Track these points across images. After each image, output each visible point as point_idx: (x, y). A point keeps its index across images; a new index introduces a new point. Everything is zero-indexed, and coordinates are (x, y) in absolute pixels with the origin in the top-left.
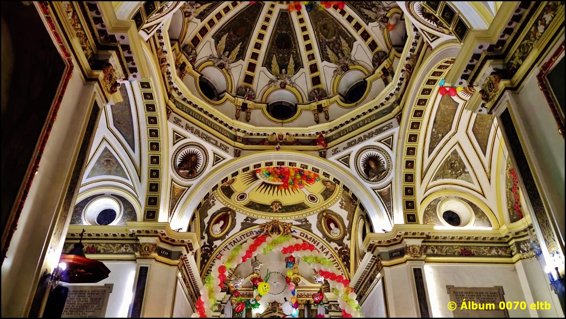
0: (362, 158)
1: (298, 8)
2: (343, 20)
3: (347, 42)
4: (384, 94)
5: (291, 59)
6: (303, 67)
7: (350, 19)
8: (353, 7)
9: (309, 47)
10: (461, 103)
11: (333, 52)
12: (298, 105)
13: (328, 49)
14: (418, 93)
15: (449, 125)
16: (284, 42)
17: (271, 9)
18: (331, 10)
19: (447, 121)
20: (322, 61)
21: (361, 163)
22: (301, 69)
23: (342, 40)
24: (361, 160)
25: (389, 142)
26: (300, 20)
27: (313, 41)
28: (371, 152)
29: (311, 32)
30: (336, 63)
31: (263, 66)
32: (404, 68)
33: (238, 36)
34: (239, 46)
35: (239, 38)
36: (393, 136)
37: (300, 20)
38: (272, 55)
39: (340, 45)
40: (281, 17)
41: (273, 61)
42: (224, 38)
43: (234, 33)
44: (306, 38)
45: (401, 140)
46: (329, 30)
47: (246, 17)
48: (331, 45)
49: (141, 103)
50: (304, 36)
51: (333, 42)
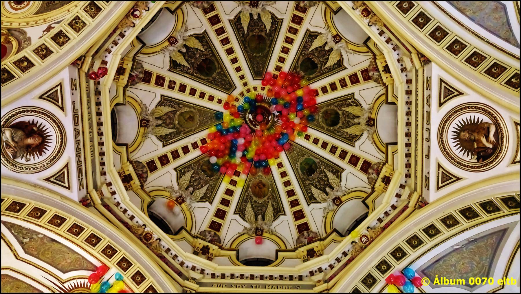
0: (48, 125)
1: (227, 106)
2: (188, 141)
4: (117, 183)
5: (186, 64)
6: (169, 70)
7: (186, 150)
8: (196, 161)
9: (182, 88)
10: (64, 277)
11: (164, 115)
12: (141, 45)
14: (127, 254)
15: (36, 253)
17: (244, 81)
18: (204, 134)
19: (43, 254)
20: (162, 96)
21: (40, 121)
22: (168, 67)
23: (171, 131)
24: (45, 123)
25: (60, 178)
27: (185, 97)
28: (53, 145)
29: (195, 100)
30: (153, 113)
31: (205, 31)
33: (253, 36)
34: (245, 28)
35: (251, 34)
36: (68, 188)
39: (167, 126)
40: (229, 83)
41: (200, 44)
42: (268, 26)
43: (260, 37)
45: (57, 199)
46: (186, 121)
47: (260, 56)
48: (171, 115)
50: (195, 90)
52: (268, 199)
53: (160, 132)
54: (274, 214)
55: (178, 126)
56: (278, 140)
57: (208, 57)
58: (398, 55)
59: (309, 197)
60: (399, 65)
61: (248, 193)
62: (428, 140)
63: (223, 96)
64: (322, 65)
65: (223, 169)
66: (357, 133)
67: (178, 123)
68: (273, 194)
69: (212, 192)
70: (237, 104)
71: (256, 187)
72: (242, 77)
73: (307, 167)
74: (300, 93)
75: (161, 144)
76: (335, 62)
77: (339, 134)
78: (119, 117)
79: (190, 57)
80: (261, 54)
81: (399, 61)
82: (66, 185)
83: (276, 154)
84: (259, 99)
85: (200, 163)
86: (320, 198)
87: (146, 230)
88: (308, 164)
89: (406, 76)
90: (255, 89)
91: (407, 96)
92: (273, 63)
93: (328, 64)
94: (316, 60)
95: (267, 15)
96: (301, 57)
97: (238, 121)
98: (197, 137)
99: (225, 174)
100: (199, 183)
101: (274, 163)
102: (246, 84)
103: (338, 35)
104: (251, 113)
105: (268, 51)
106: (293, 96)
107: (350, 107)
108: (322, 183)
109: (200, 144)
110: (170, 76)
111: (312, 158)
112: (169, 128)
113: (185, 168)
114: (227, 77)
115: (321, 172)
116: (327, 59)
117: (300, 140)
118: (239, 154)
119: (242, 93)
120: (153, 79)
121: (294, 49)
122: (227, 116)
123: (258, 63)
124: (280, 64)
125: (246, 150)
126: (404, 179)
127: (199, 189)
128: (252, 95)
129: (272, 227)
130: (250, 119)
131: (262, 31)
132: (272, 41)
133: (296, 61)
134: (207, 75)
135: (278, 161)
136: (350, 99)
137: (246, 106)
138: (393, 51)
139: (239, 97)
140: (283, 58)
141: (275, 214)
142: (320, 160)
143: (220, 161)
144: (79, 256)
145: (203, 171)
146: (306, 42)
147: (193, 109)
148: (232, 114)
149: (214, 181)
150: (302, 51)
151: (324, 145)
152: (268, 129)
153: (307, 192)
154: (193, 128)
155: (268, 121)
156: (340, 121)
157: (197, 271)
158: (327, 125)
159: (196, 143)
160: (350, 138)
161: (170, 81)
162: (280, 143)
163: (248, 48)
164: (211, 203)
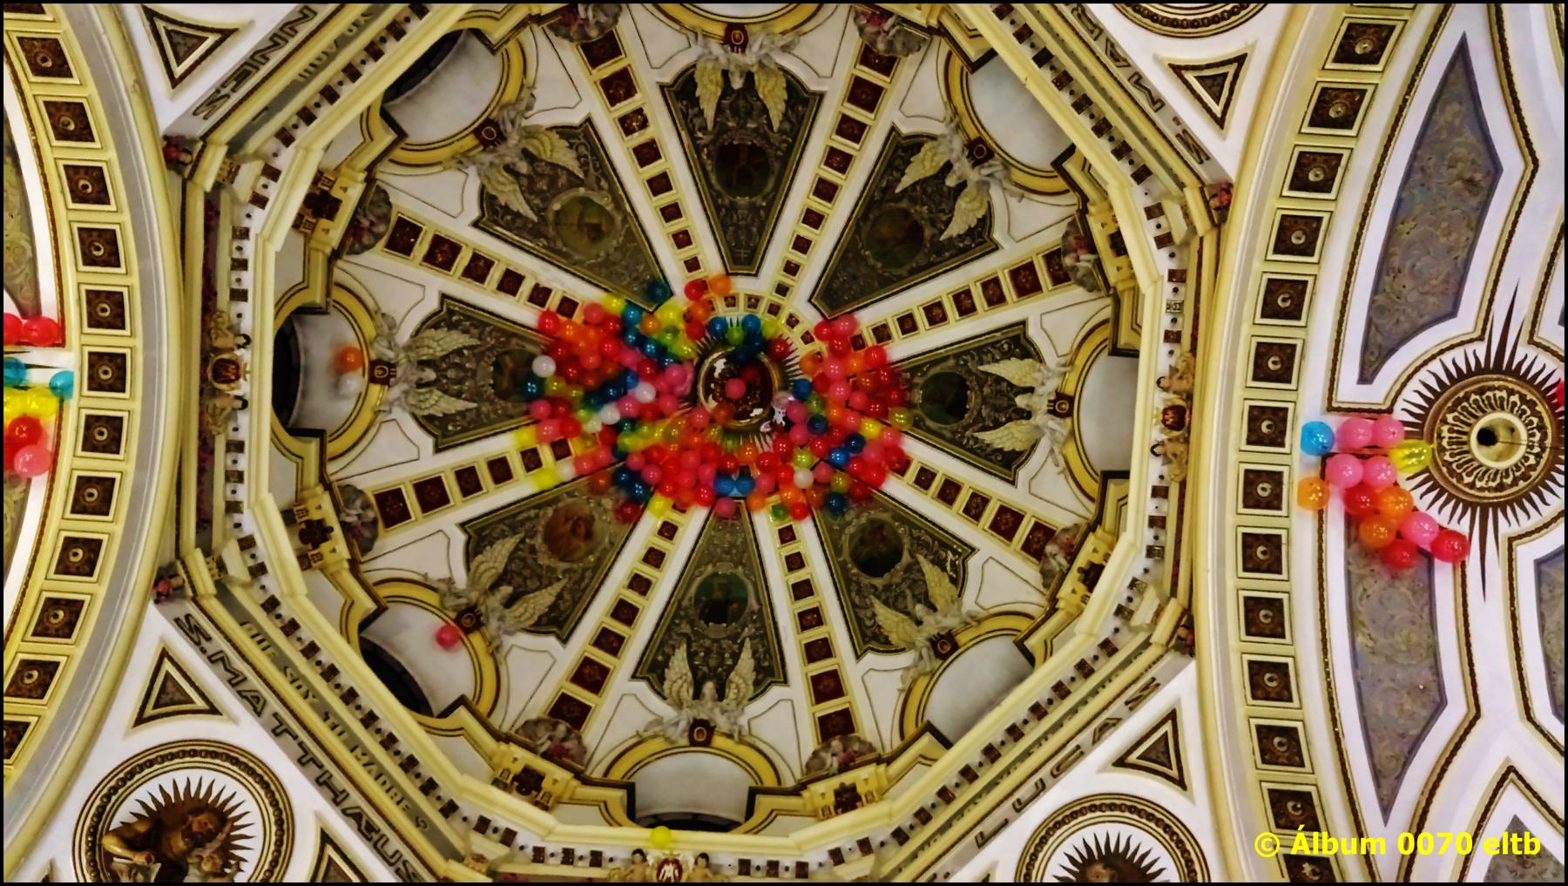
1: (697, 289)
2: (536, 270)
3: (506, 208)
4: (293, 185)
5: (709, 111)
6: (662, 87)
8: (506, 330)
9: (646, 153)
11: (548, 164)
13: (573, 165)
14: (140, 359)
16: (744, 161)
17: (787, 280)
18: (585, 293)
20: (589, 120)
22: (668, 80)
23: (525, 210)
26: (689, 242)
29: (646, 207)
30: (531, 133)
31: (821, 96)
32: (244, 355)
33: (906, 213)
34: (907, 181)
35: (904, 204)
36: (175, 82)
37: (689, 242)
38: (787, 126)
39: (529, 190)
40: (754, 250)
41: (782, 107)
42: (956, 228)
43: (916, 229)
44: (660, 184)
45: (123, 77)
46: (580, 225)
47: (873, 268)
48: (563, 180)
49: (1326, 274)
50: (668, 188)
51: (560, 191)
52: (565, 572)
53: (501, 188)
54: (540, 617)
55: (550, 216)
56: (722, 474)
57: (770, 151)
58: (1146, 571)
59: (654, 661)
60: (1127, 593)
61: (537, 516)
62: (1020, 807)
63: (712, 263)
64: (975, 423)
65: (542, 408)
66: (893, 638)
67: (557, 213)
68: (588, 574)
69: (465, 430)
70: (721, 309)
71: (567, 520)
72: (791, 269)
73: (718, 595)
74: (871, 429)
75: (474, 213)
76: (1008, 447)
77: (857, 600)
78: (453, 61)
79: (735, 112)
80: (879, 265)
81: (1133, 584)
82: (179, 71)
83: (686, 497)
84: (778, 350)
85: (508, 342)
86: (675, 688)
87: (239, 352)
88: (728, 592)
89: (1117, 630)
90: (792, 322)
91: (1072, 673)
92: (883, 311)
93: (987, 437)
94: (973, 400)
95: (976, 204)
96: (951, 362)
97: (685, 348)
98: (563, 284)
99: (536, 422)
100: (460, 381)
101: (661, 513)
102: (784, 290)
103: (1071, 400)
104: (729, 358)
105: (900, 279)
106: (851, 420)
107: (937, 570)
108: (712, 663)
109: (553, 303)
110: (648, 98)
111: (750, 588)
112: (528, 202)
113: (468, 318)
114: (760, 234)
115: (734, 638)
116: (997, 425)
117: (765, 525)
118: (611, 414)
119: (758, 299)
120: (609, 69)
121: (958, 329)
122: (673, 311)
123: (855, 278)
124: (895, 329)
125: (633, 421)
126: (885, 835)
127: (445, 392)
128: (773, 326)
129: (508, 641)
130: (712, 369)
131: (933, 224)
132: (930, 265)
133: (935, 358)
134: (727, 185)
135: (675, 517)
136: (955, 552)
137: (736, 335)
138: (1144, 552)
139: (742, 302)
140: (915, 322)
141: (545, 620)
142: (760, 610)
143: (555, 386)
144: (28, 247)
145: (496, 365)
146: (993, 345)
147: (619, 218)
148: (688, 317)
149: (495, 411)
150: (967, 352)
151: (802, 590)
152: (727, 432)
153: (662, 644)
154: (577, 257)
155: (746, 414)
156: (887, 576)
157: (247, 557)
158: (854, 556)
159: (548, 291)
160: (869, 632)
161: (639, 111)
162: (723, 486)
163: (869, 224)
164: (438, 449)
